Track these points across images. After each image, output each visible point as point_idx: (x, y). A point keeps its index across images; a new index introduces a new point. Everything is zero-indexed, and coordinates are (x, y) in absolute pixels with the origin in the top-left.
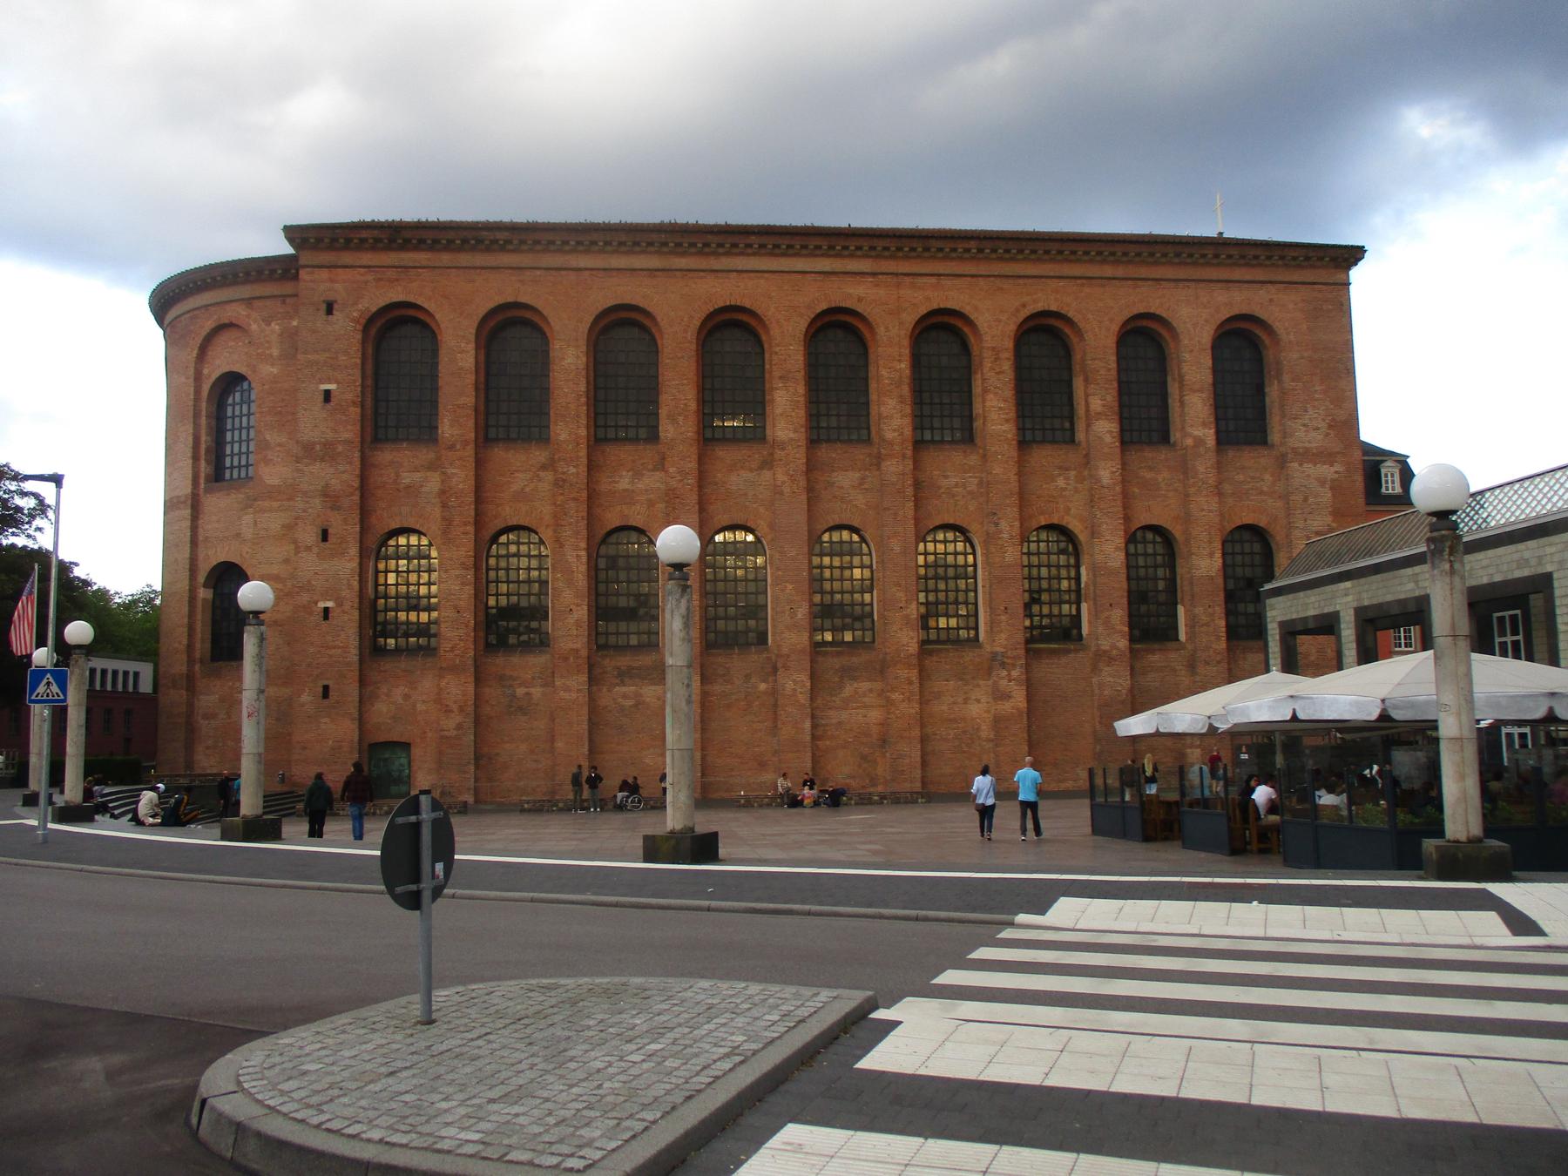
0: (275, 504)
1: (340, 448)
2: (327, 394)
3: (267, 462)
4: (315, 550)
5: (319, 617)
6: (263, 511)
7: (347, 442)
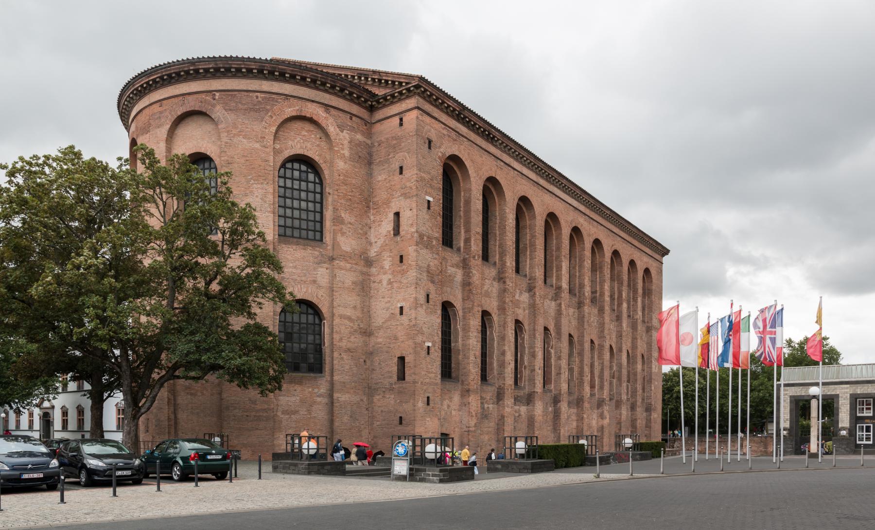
0: (348, 266)
1: (434, 243)
2: (429, 201)
3: (343, 234)
4: (424, 307)
5: (424, 353)
6: (341, 269)
7: (436, 238)
